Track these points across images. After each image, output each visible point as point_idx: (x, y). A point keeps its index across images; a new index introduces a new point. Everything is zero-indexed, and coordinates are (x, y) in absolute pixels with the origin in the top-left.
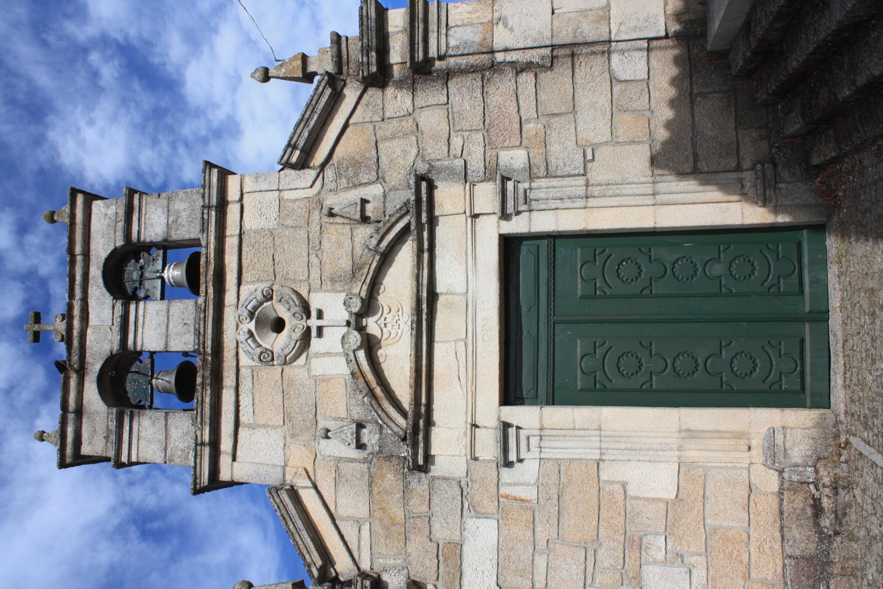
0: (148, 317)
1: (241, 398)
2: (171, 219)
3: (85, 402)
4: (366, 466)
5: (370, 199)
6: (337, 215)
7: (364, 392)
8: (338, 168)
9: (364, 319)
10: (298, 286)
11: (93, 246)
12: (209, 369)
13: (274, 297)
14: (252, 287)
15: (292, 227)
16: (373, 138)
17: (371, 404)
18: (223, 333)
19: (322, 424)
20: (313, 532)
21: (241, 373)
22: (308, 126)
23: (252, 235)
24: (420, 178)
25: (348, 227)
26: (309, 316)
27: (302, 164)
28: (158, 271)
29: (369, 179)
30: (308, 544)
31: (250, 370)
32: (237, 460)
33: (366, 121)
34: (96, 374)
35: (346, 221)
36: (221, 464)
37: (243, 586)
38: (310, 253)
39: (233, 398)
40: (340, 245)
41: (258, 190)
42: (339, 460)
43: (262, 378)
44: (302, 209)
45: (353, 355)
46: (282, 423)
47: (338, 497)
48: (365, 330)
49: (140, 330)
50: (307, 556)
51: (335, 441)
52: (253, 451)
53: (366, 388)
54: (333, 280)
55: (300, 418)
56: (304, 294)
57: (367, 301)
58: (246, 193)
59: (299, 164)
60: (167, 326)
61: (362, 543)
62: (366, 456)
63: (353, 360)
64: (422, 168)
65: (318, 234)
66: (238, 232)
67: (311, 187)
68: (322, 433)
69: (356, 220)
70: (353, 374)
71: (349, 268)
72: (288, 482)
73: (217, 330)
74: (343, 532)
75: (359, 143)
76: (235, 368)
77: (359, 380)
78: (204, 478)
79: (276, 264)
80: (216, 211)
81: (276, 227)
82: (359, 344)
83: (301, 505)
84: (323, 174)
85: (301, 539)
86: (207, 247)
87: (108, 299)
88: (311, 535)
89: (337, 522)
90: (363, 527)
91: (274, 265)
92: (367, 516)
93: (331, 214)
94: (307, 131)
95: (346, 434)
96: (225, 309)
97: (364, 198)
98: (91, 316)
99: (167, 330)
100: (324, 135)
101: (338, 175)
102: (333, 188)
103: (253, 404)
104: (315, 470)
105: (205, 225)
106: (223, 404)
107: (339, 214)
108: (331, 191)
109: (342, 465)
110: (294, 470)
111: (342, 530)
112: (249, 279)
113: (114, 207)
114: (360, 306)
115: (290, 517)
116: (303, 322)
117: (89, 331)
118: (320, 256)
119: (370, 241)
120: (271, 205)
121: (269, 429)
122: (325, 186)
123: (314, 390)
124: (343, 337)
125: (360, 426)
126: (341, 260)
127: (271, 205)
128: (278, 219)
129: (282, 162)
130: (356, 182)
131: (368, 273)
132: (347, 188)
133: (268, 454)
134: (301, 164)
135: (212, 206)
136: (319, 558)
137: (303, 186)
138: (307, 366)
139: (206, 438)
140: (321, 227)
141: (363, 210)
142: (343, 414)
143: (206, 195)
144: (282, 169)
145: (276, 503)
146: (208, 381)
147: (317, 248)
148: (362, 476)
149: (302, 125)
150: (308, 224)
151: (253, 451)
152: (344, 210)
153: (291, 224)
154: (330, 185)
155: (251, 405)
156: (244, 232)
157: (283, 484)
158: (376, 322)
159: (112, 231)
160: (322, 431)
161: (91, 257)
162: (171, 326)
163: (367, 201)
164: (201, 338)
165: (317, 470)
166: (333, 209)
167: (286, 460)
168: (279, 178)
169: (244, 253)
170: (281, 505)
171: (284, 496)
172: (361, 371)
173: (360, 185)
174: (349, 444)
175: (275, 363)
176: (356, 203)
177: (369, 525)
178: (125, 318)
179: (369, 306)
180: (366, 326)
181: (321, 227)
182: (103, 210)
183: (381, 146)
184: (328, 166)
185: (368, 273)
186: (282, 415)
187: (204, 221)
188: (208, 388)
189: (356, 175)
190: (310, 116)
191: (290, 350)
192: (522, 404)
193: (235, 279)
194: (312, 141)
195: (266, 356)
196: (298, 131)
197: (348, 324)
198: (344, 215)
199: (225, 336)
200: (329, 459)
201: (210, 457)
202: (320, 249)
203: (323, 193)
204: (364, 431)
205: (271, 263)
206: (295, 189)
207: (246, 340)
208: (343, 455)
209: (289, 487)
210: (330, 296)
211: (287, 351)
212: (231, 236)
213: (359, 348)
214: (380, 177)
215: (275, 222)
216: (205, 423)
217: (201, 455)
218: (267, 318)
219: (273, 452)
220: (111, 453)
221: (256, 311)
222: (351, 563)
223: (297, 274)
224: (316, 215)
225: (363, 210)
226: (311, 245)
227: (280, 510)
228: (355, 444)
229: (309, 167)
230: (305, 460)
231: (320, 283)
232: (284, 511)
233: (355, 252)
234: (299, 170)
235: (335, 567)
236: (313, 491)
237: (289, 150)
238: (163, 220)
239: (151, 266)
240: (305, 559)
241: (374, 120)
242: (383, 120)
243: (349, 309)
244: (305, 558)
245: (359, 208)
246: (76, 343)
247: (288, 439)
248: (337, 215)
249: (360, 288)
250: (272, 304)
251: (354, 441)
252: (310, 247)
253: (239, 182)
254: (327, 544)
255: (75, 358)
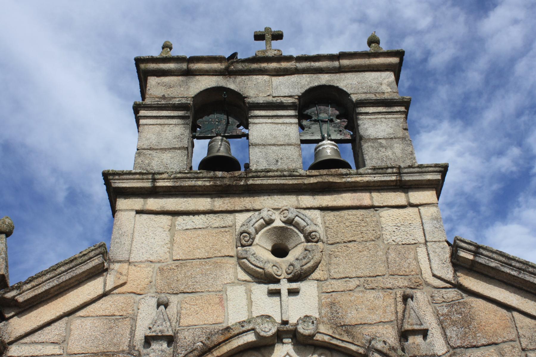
0: (283, 127)
1: (202, 216)
2: (384, 142)
3: (197, 77)
4: (126, 348)
5: (428, 340)
6: (405, 305)
7: (208, 342)
8: (459, 302)
9: (290, 340)
10: (324, 268)
11: (349, 75)
12: (231, 183)
13: (309, 244)
14: (319, 221)
15: (387, 258)
16: (500, 340)
17: (194, 350)
18: (269, 196)
19: (174, 300)
20: (56, 293)
21: (228, 215)
22: (502, 266)
23: (374, 219)
25: (393, 318)
26: (290, 280)
28: (329, 135)
29: (451, 337)
30: (42, 286)
31: (231, 223)
32: (138, 215)
33: (519, 331)
34: (225, 85)
35: (400, 315)
36: (134, 199)
37: (8, 226)
38: (360, 279)
39: (201, 208)
40: (372, 309)
41: (424, 221)
42: (134, 319)
43: (223, 236)
44: (408, 267)
45: (250, 328)
46: (175, 258)
47: (93, 318)
48: (278, 343)
49: (270, 121)
50: (29, 286)
51: (154, 314)
52: (146, 230)
53: (213, 344)
54: (332, 305)
55: (180, 277)
56: (316, 275)
57: (310, 342)
58: (419, 210)
59: (458, 260)
60: (274, 145)
61: (40, 347)
62: (136, 348)
63: (244, 329)
65: (382, 286)
66: (376, 204)
67: (434, 276)
68: (164, 297)
69: (402, 326)
70: (228, 329)
71: (347, 322)
72: (112, 266)
73: (273, 190)
74: (53, 326)
75: (492, 324)
76: (233, 209)
77: (221, 336)
78: (119, 183)
79: (345, 244)
80: (396, 181)
81: (386, 242)
82: (262, 334)
83: (86, 280)
84: (450, 288)
85: (49, 279)
86: (358, 174)
87: (298, 91)
88: (52, 290)
89: (66, 318)
90: (57, 347)
91: (345, 242)
92: (69, 351)
93: (406, 298)
94: (497, 265)
95: (162, 325)
96: (295, 197)
97: (429, 333)
98: (281, 78)
99: (270, 145)
100: (495, 285)
101: (451, 304)
102: (436, 299)
103: (195, 228)
104: (123, 293)
105: (380, 171)
106: (195, 199)
107: (407, 306)
108: (432, 297)
109: (127, 322)
110: (124, 272)
111: (56, 324)
112: (327, 218)
113: (389, 90)
114: (304, 333)
115: (73, 267)
116: (284, 275)
117: (266, 78)
118: (358, 289)
119: (379, 341)
120: (408, 235)
121: (169, 245)
122: (436, 290)
123: (210, 290)
124: (269, 317)
125: (170, 340)
126: (355, 311)
127: (408, 235)
128: (394, 243)
129: (458, 241)
130: (446, 324)
131: (343, 341)
132: (437, 315)
133: (143, 245)
134: (458, 263)
135: (401, 177)
136: (26, 298)
137: (435, 266)
138: (236, 281)
139: (160, 184)
140: (390, 289)
141: (414, 332)
142: (184, 322)
143: (412, 170)
144: (449, 244)
145: (90, 252)
146: (218, 183)
147: (366, 286)
148: (115, 345)
149: (503, 259)
150: (391, 275)
151: (146, 230)
152: (412, 312)
153: (390, 257)
154: (438, 295)
155: (195, 227)
156: (376, 210)
157: (110, 261)
158: (288, 354)
159: (365, 91)
160: (165, 299)
161: (338, 75)
162: (274, 148)
163: (425, 336)
164: (262, 174)
165: (124, 296)
166: (412, 300)
167: (136, 264)
168: (439, 241)
169: (354, 212)
170: (86, 258)
171: (97, 261)
172: (231, 337)
173: (443, 328)
174: (150, 328)
175: (239, 248)
176: (421, 324)
177: (59, 353)
178: (281, 106)
180: (283, 343)
181: (390, 289)
182: (385, 81)
183: (492, 349)
184: (460, 292)
185: (343, 341)
186: (184, 258)
187: (385, 170)
188: (211, 183)
189: (454, 323)
190: (514, 267)
191: (253, 263)
193: (327, 204)
194: (486, 273)
195: (247, 239)
196: (495, 256)
197: (285, 323)
198: (407, 312)
199: (266, 197)
200: (135, 308)
201: (141, 188)
202: (365, 288)
203: (429, 289)
204: (165, 345)
205: (346, 240)
206: (429, 259)
207: (262, 218)
208: (139, 322)
209: (106, 267)
210: (315, 302)
211: (252, 259)
212: (372, 198)
213: (257, 334)
214: (455, 350)
215: (390, 241)
216: (175, 181)
217: (143, 179)
218: (288, 238)
219: (144, 251)
220: (148, 101)
221: (294, 226)
222: (18, 334)
223: (336, 267)
224: (402, 282)
225: (414, 332)
226: (370, 279)
227: (81, 257)
228: (150, 334)
229: (455, 271)
230: (135, 283)
231: (328, 291)
232: (80, 260)
233: (366, 327)
234: (452, 262)
235: (15, 318)
236: (100, 292)
237: (472, 248)
238: (381, 135)
239: (334, 129)
240: (26, 283)
241: (521, 340)
242: (523, 350)
243: (301, 321)
244: (28, 283)
245: (416, 327)
246: (255, 66)
247: (159, 265)
248: (405, 305)
250: (303, 242)
251: (154, 334)
252: (367, 278)
253: (429, 202)
254: (42, 308)
255: (240, 66)
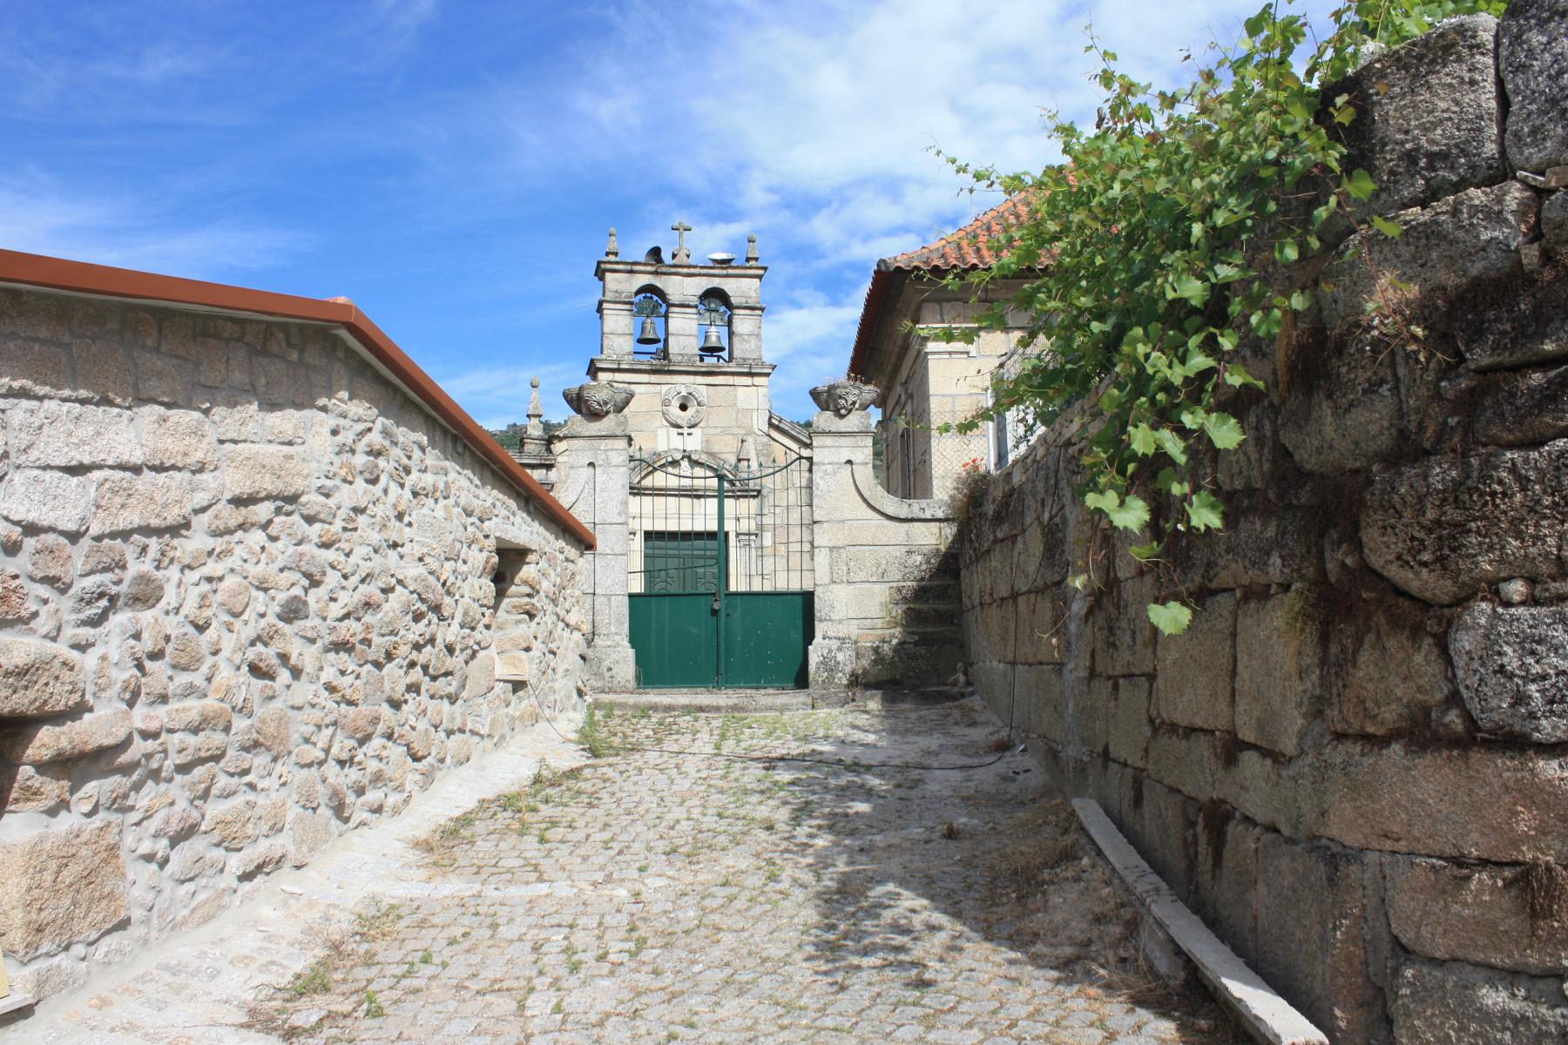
11: (732, 280)
14: (705, 394)
24: (759, 492)
27: (771, 425)
54: (707, 441)
64: (765, 492)
87: (700, 292)
93: (743, 441)
139: (622, 366)
179: (695, 463)
192: (646, 540)
220: (609, 296)
224: (743, 431)
249: (703, 458)
255: (664, 270)
